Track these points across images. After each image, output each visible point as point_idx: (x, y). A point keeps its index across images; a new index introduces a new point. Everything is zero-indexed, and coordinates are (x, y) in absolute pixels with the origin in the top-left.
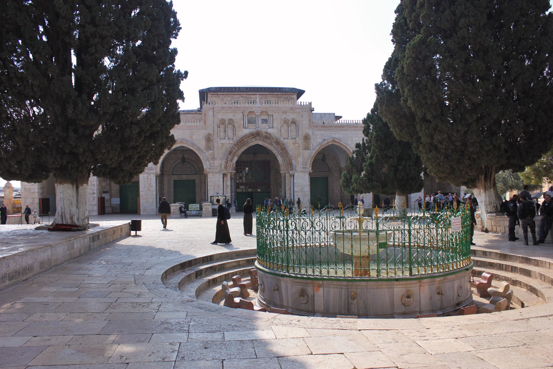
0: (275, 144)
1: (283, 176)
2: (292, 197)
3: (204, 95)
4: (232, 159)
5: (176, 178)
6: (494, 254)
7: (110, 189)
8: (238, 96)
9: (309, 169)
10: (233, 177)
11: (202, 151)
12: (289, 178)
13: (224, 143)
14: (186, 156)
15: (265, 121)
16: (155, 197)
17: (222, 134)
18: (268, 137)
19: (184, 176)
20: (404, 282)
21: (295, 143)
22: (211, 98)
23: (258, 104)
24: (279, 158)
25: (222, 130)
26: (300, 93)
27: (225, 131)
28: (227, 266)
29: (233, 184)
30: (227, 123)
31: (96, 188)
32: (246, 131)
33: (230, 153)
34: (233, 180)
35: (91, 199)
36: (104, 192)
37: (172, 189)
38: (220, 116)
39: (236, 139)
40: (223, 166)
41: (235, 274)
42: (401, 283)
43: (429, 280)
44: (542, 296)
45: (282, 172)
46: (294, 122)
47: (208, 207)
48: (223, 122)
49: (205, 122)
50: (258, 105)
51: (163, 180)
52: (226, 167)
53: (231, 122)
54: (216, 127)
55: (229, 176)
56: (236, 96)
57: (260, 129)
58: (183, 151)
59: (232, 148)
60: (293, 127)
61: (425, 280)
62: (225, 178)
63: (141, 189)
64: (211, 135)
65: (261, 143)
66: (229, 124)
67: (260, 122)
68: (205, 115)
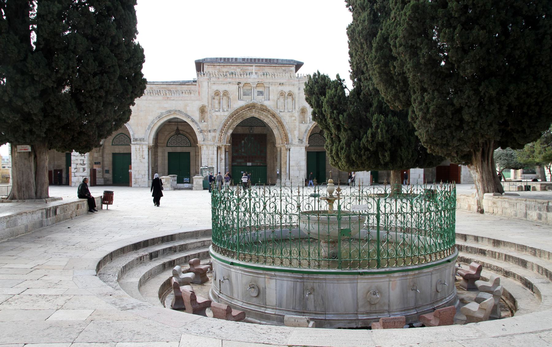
0: (271, 117)
1: (279, 150)
2: (288, 172)
3: (199, 65)
4: (227, 131)
5: (170, 150)
6: (487, 240)
7: (103, 161)
8: (235, 67)
9: (306, 143)
10: (227, 150)
11: (196, 123)
12: (285, 152)
13: (220, 116)
14: (180, 128)
15: (260, 93)
16: (147, 169)
17: (217, 106)
18: (264, 109)
19: (178, 148)
20: (370, 276)
21: (291, 116)
22: (206, 68)
23: (254, 76)
24: (276, 132)
25: (216, 101)
26: (298, 65)
28: (189, 246)
29: (227, 157)
30: (221, 95)
31: (86, 159)
32: (242, 103)
33: (225, 125)
34: (227, 153)
35: (81, 170)
36: (95, 163)
37: (166, 162)
38: (215, 88)
39: (231, 111)
40: (217, 139)
41: (194, 256)
42: (366, 277)
43: (401, 274)
44: (539, 295)
46: (290, 94)
47: (198, 180)
48: (217, 93)
49: (199, 93)
50: (254, 76)
51: (157, 152)
52: (220, 140)
55: (223, 149)
56: (232, 67)
57: (255, 101)
58: (178, 122)
59: (228, 121)
60: (290, 100)
61: (396, 275)
62: (219, 151)
63: (132, 161)
64: (205, 107)
65: (256, 115)
66: (224, 95)
68: (199, 86)
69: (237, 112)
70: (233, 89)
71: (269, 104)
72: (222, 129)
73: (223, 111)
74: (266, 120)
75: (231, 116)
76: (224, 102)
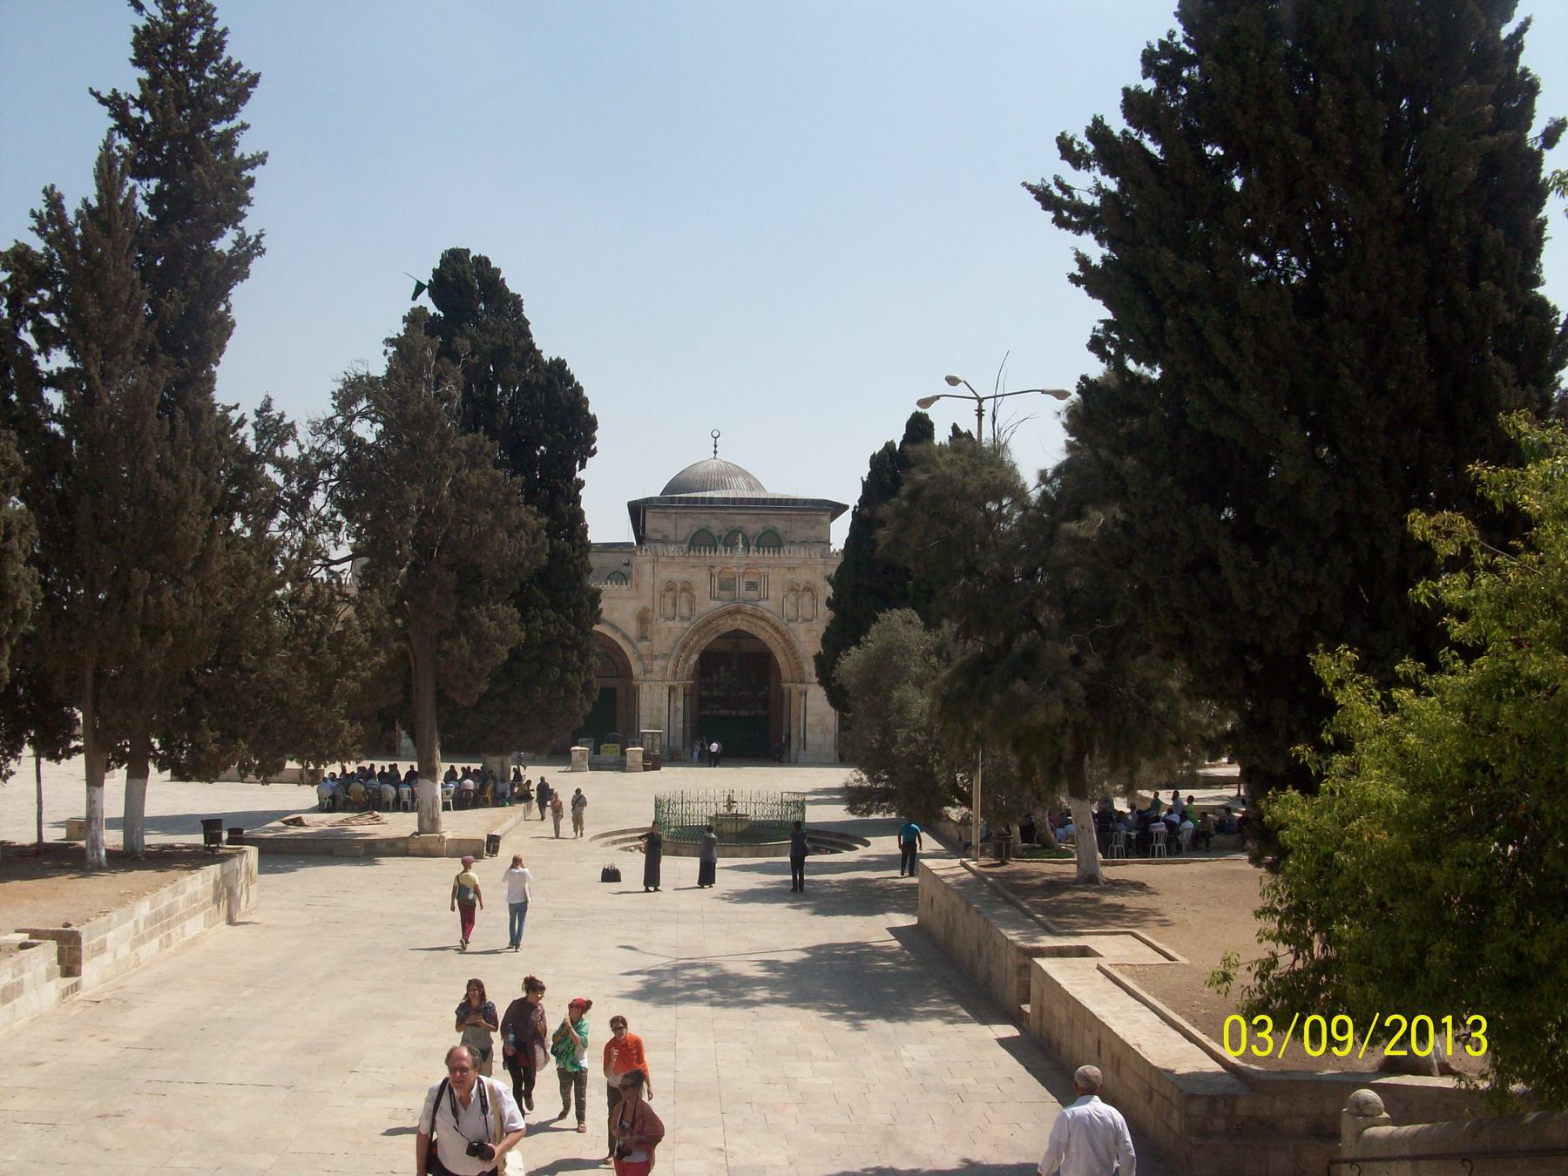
3: (638, 511)
4: (688, 657)
15: (752, 586)
17: (669, 611)
24: (781, 659)
27: (674, 605)
33: (684, 647)
45: (785, 685)
46: (808, 589)
48: (670, 587)
53: (687, 588)
54: (657, 596)
55: (680, 690)
60: (807, 598)
66: (684, 590)
67: (743, 587)
69: (707, 623)
70: (699, 578)
71: (769, 606)
72: (679, 657)
73: (682, 619)
74: (762, 636)
75: (696, 631)
76: (683, 600)
